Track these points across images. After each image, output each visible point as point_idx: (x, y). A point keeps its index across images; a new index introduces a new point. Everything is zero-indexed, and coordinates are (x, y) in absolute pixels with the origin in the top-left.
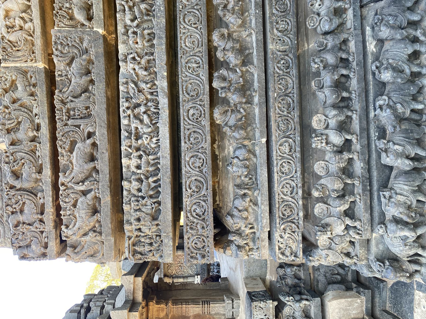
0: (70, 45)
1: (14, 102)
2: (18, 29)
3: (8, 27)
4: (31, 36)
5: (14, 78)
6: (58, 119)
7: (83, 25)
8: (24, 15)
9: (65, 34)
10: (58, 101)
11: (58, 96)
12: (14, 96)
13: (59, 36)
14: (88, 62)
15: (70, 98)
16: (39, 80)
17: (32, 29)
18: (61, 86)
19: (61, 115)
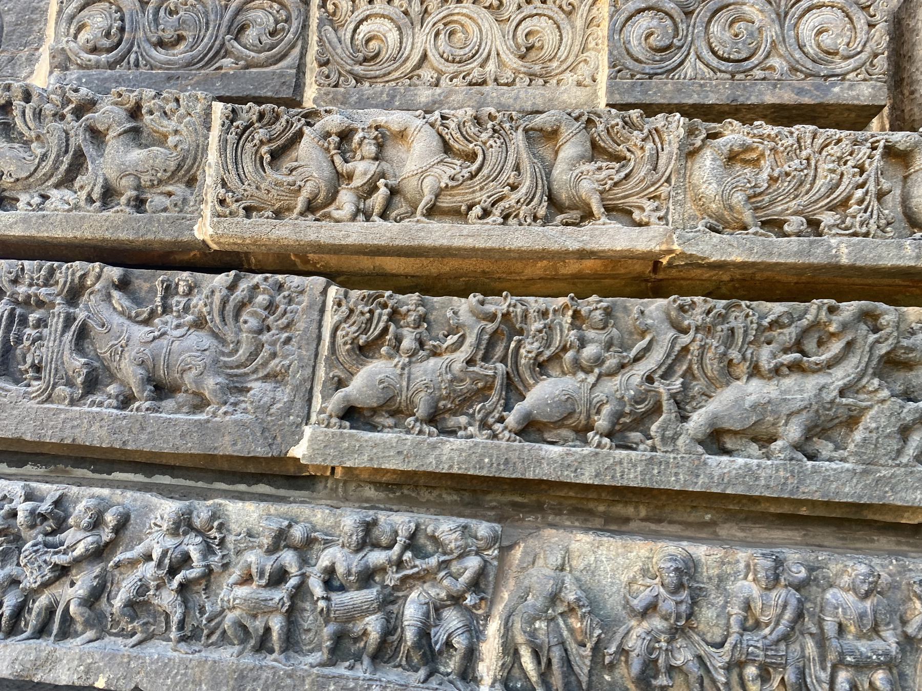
0: (265, 337)
1: (96, 135)
2: (339, 168)
3: (345, 135)
4: (311, 208)
5: (172, 140)
6: (23, 269)
7: (340, 384)
8: (383, 191)
9: (301, 325)
10: (78, 274)
11: (98, 277)
12: (111, 134)
13: (299, 303)
14: (194, 393)
15: (81, 314)
16: (151, 220)
17: (336, 214)
18: (146, 286)
19: (32, 279)
